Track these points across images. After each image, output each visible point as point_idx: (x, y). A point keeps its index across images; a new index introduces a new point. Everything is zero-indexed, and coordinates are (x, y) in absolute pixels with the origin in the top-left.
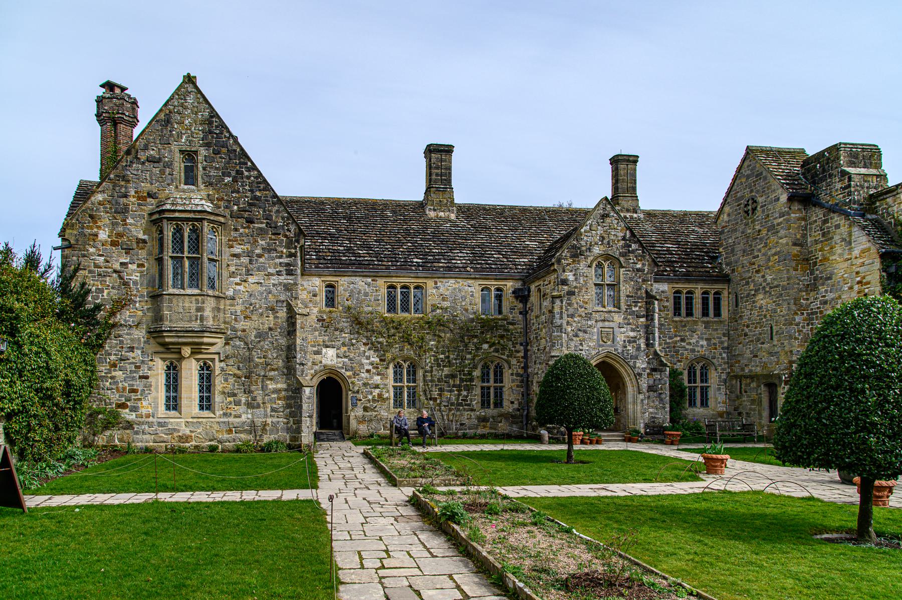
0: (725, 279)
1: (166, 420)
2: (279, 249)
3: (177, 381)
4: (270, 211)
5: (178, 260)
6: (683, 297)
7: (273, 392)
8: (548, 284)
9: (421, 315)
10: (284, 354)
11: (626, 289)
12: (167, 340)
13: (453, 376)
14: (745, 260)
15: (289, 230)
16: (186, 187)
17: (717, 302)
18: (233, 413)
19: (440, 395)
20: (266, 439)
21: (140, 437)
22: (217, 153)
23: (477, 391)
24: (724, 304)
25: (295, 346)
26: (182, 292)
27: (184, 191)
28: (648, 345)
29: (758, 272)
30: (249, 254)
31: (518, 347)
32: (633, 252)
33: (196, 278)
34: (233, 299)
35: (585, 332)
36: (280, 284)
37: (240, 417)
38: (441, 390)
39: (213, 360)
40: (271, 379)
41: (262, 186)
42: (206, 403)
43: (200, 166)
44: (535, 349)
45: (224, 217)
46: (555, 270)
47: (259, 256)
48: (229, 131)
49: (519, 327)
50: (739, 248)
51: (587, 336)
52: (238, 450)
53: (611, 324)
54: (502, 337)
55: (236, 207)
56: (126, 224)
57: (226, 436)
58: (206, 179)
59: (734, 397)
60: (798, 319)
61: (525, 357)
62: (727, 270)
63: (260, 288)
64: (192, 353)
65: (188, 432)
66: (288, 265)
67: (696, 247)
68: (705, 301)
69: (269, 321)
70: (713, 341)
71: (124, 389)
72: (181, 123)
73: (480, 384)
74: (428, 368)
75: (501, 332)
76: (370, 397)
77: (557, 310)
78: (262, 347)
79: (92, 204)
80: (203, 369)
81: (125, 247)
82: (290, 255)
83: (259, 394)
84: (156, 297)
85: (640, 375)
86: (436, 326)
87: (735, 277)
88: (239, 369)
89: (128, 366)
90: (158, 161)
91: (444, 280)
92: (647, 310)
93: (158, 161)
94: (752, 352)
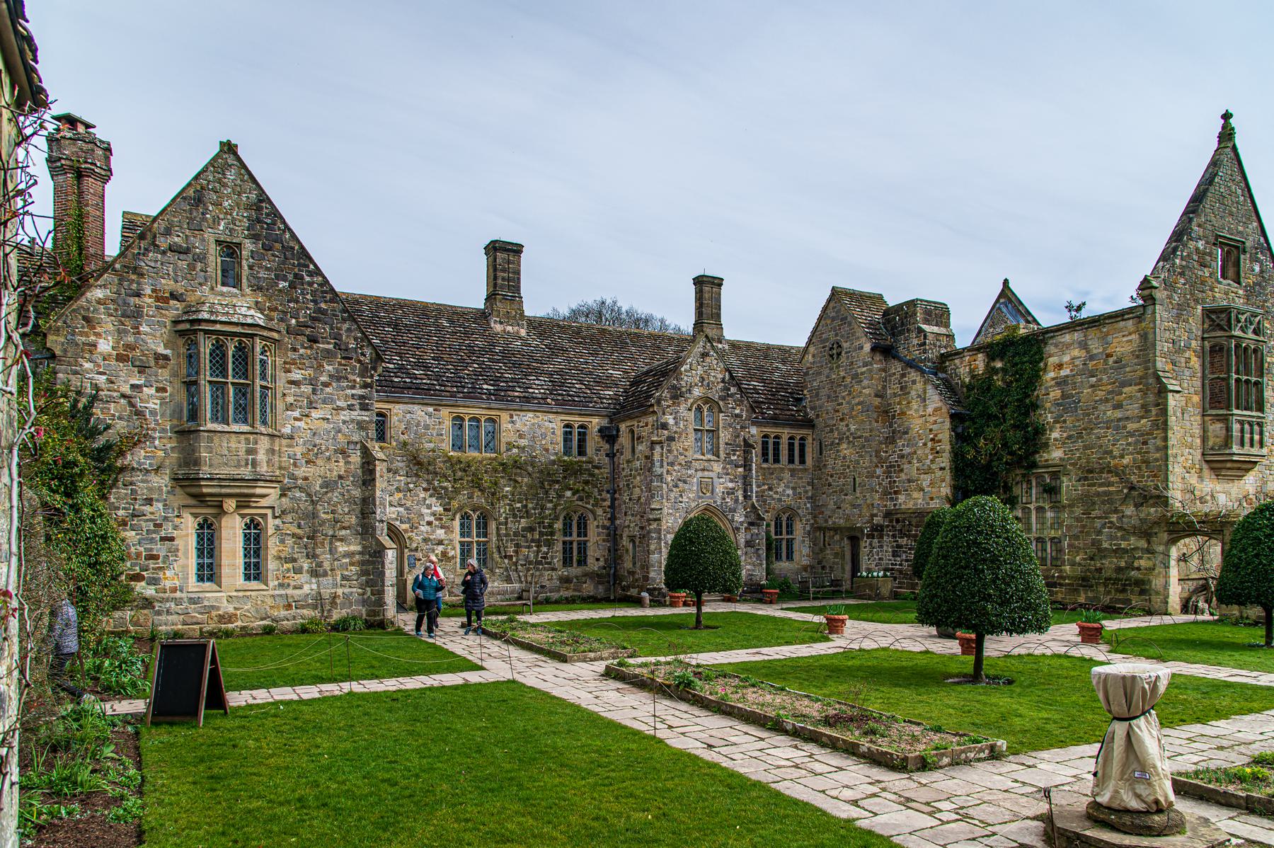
0: (809, 424)
1: (201, 595)
2: (351, 377)
3: (212, 543)
4: (340, 329)
5: (219, 387)
6: (771, 441)
7: (344, 556)
8: (645, 426)
9: (494, 455)
10: (358, 508)
11: (725, 436)
12: (205, 490)
13: (531, 529)
14: (830, 406)
15: (363, 354)
16: (225, 289)
17: (802, 447)
19: (516, 552)
20: (336, 615)
21: (163, 618)
22: (267, 248)
23: (559, 547)
24: (808, 450)
25: (374, 499)
26: (226, 428)
27: (223, 294)
28: (745, 497)
29: (842, 420)
30: (312, 382)
31: (604, 494)
32: (732, 395)
33: (244, 413)
34: (292, 438)
35: (685, 482)
36: (353, 421)
37: (301, 587)
38: (517, 546)
39: (264, 516)
40: (341, 540)
41: (328, 296)
42: (254, 571)
43: (244, 262)
44: (626, 498)
45: (279, 332)
46: (654, 412)
47: (326, 385)
48: (284, 222)
49: (606, 471)
50: (824, 392)
51: (686, 486)
52: (304, 630)
54: (587, 482)
55: (294, 321)
56: (139, 333)
57: (283, 613)
59: (818, 550)
61: (612, 506)
62: (811, 414)
63: (326, 426)
64: (238, 507)
65: (231, 609)
66: (362, 397)
67: (782, 386)
68: (791, 446)
69: (340, 467)
70: (799, 490)
71: (138, 555)
72: (218, 204)
73: (562, 538)
74: (502, 519)
75: (585, 477)
77: (657, 457)
79: (88, 301)
80: (249, 528)
81: (137, 363)
82: (365, 386)
83: (326, 559)
84: (187, 434)
85: (738, 529)
86: (511, 468)
87: (819, 422)
88: (299, 527)
89: (144, 524)
90: (186, 251)
92: (745, 459)
93: (186, 251)
94: (835, 503)
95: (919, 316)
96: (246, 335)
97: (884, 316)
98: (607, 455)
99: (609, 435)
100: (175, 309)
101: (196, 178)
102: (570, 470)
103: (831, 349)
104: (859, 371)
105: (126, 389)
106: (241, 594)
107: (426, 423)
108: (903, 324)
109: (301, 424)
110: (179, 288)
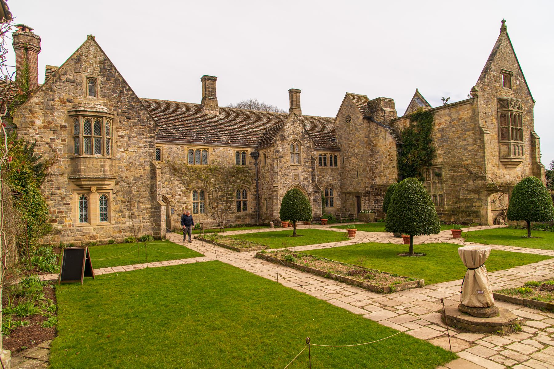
0: (338, 150)
1: (82, 228)
3: (86, 205)
5: (88, 139)
6: (323, 157)
7: (143, 210)
8: (270, 152)
10: (149, 189)
11: (303, 155)
12: (83, 183)
13: (223, 196)
14: (347, 142)
16: (90, 97)
17: (336, 159)
18: (121, 222)
19: (217, 206)
20: (141, 235)
23: (235, 203)
24: (338, 160)
25: (156, 185)
26: (92, 156)
27: (89, 100)
28: (313, 181)
29: (352, 148)
32: (306, 138)
33: (99, 149)
34: (120, 160)
35: (287, 175)
38: (217, 203)
39: (109, 193)
40: (142, 203)
42: (105, 217)
43: (99, 86)
44: (263, 182)
45: (114, 115)
46: (274, 146)
47: (134, 137)
48: (115, 69)
50: (344, 136)
51: (288, 177)
52: (127, 242)
53: (298, 171)
54: (246, 176)
56: (53, 116)
57: (118, 235)
58: (103, 94)
59: (343, 202)
60: (367, 169)
61: (257, 186)
62: (339, 146)
63: (135, 154)
64: (97, 190)
66: (150, 142)
67: (327, 134)
68: (331, 159)
69: (141, 172)
73: (236, 200)
74: (211, 192)
75: (245, 174)
76: (181, 209)
77: (275, 165)
78: (137, 186)
80: (102, 198)
81: (53, 129)
82: (151, 137)
83: (136, 211)
84: (75, 159)
85: (310, 194)
86: (214, 171)
88: (124, 198)
90: (73, 82)
92: (312, 164)
93: (73, 82)
95: (382, 104)
96: (100, 117)
97: (368, 104)
99: (255, 156)
100: (69, 106)
101: (78, 50)
102: (239, 171)
104: (358, 127)
105: (48, 140)
106: (99, 227)
107: (177, 153)
108: (375, 108)
109: (124, 154)
110: (71, 97)
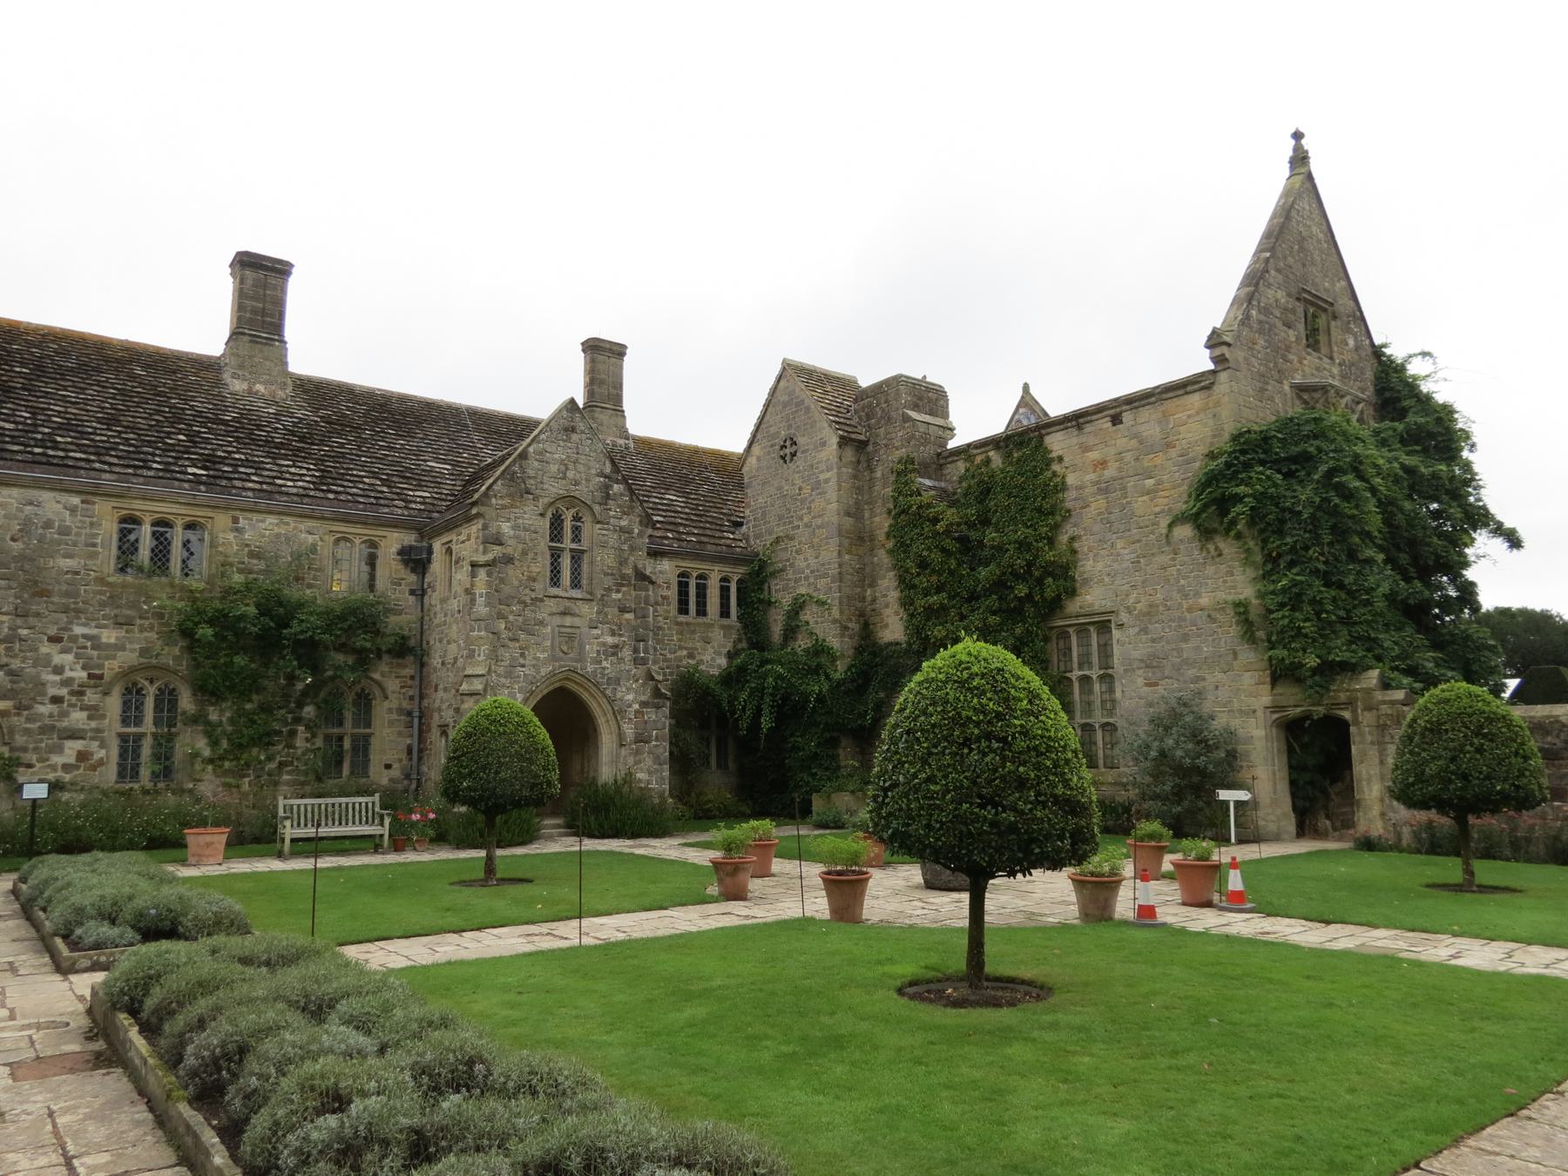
53: (577, 621)
91: (255, 517)
98: (412, 592)
103: (783, 447)
104: (822, 477)
